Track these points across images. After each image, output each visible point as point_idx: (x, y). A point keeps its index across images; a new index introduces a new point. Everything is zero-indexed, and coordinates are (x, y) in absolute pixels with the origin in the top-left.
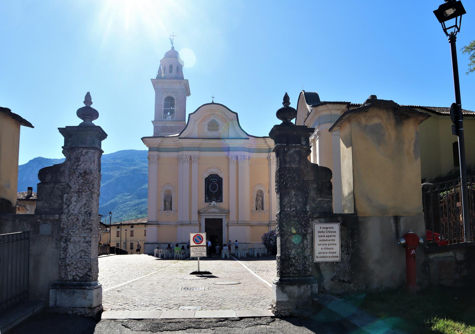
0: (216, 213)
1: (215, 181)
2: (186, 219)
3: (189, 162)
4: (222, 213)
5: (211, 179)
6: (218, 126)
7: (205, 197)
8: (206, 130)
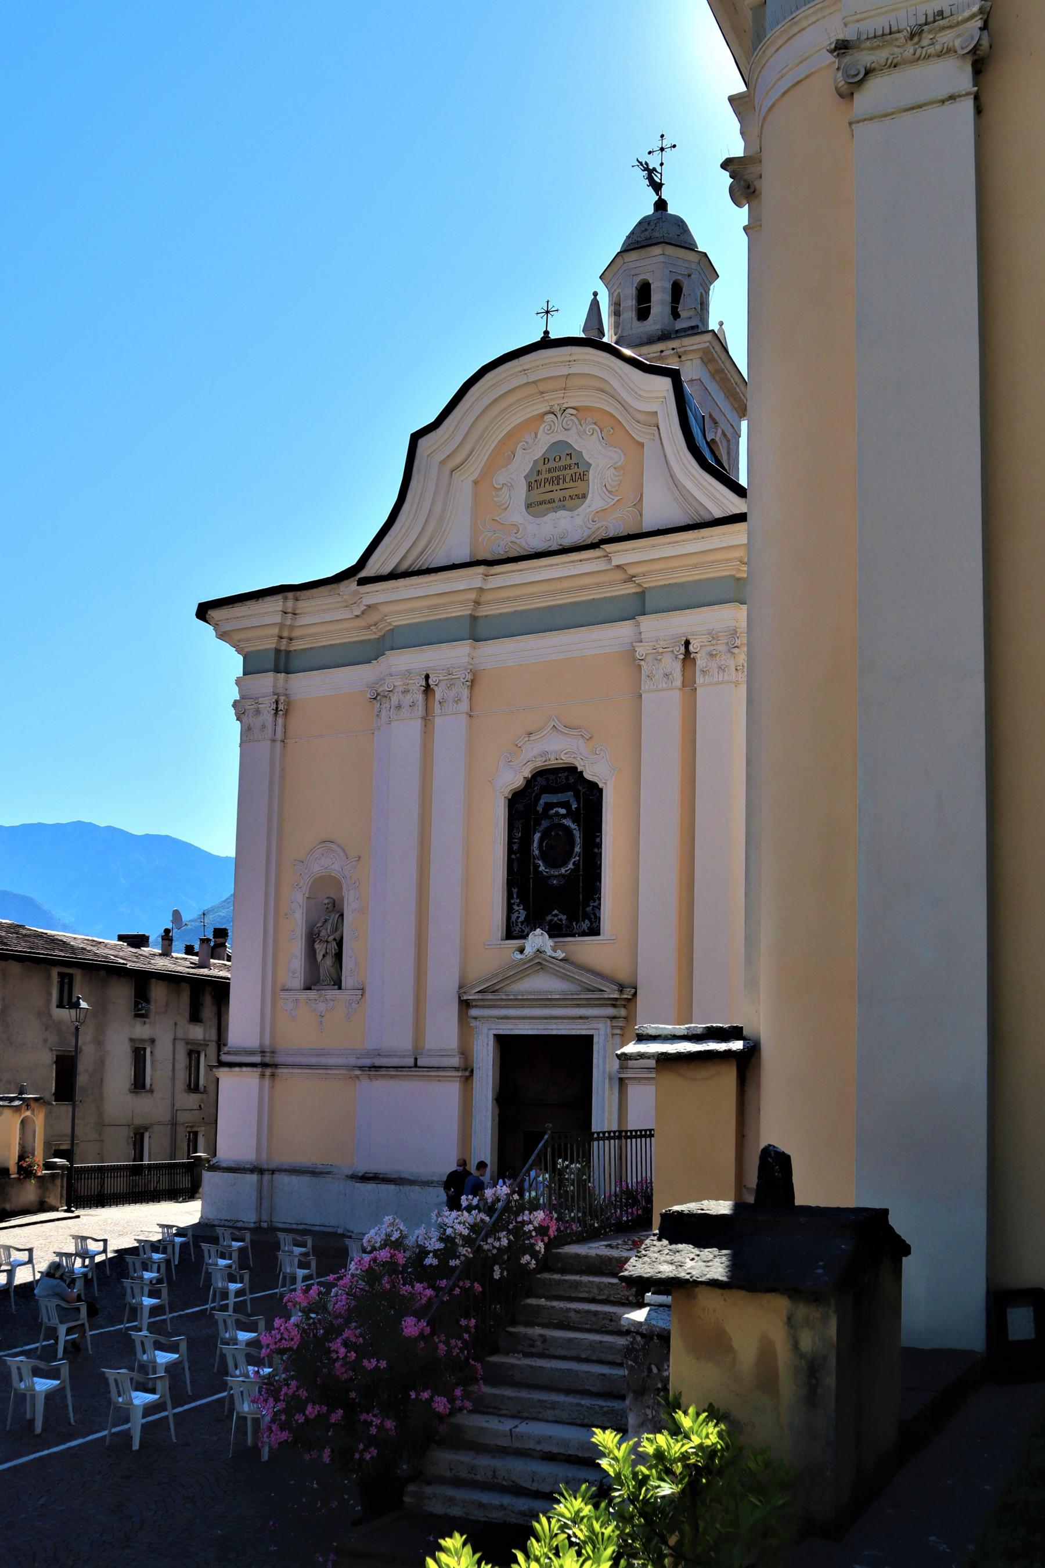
0: (548, 1002)
1: (566, 805)
2: (398, 1040)
3: (420, 711)
4: (589, 1004)
5: (542, 802)
6: (583, 477)
7: (510, 910)
8: (518, 515)
